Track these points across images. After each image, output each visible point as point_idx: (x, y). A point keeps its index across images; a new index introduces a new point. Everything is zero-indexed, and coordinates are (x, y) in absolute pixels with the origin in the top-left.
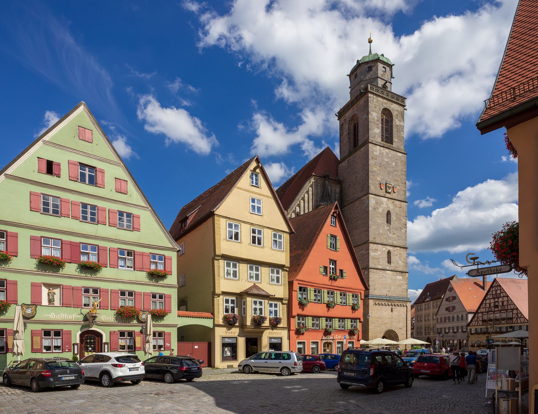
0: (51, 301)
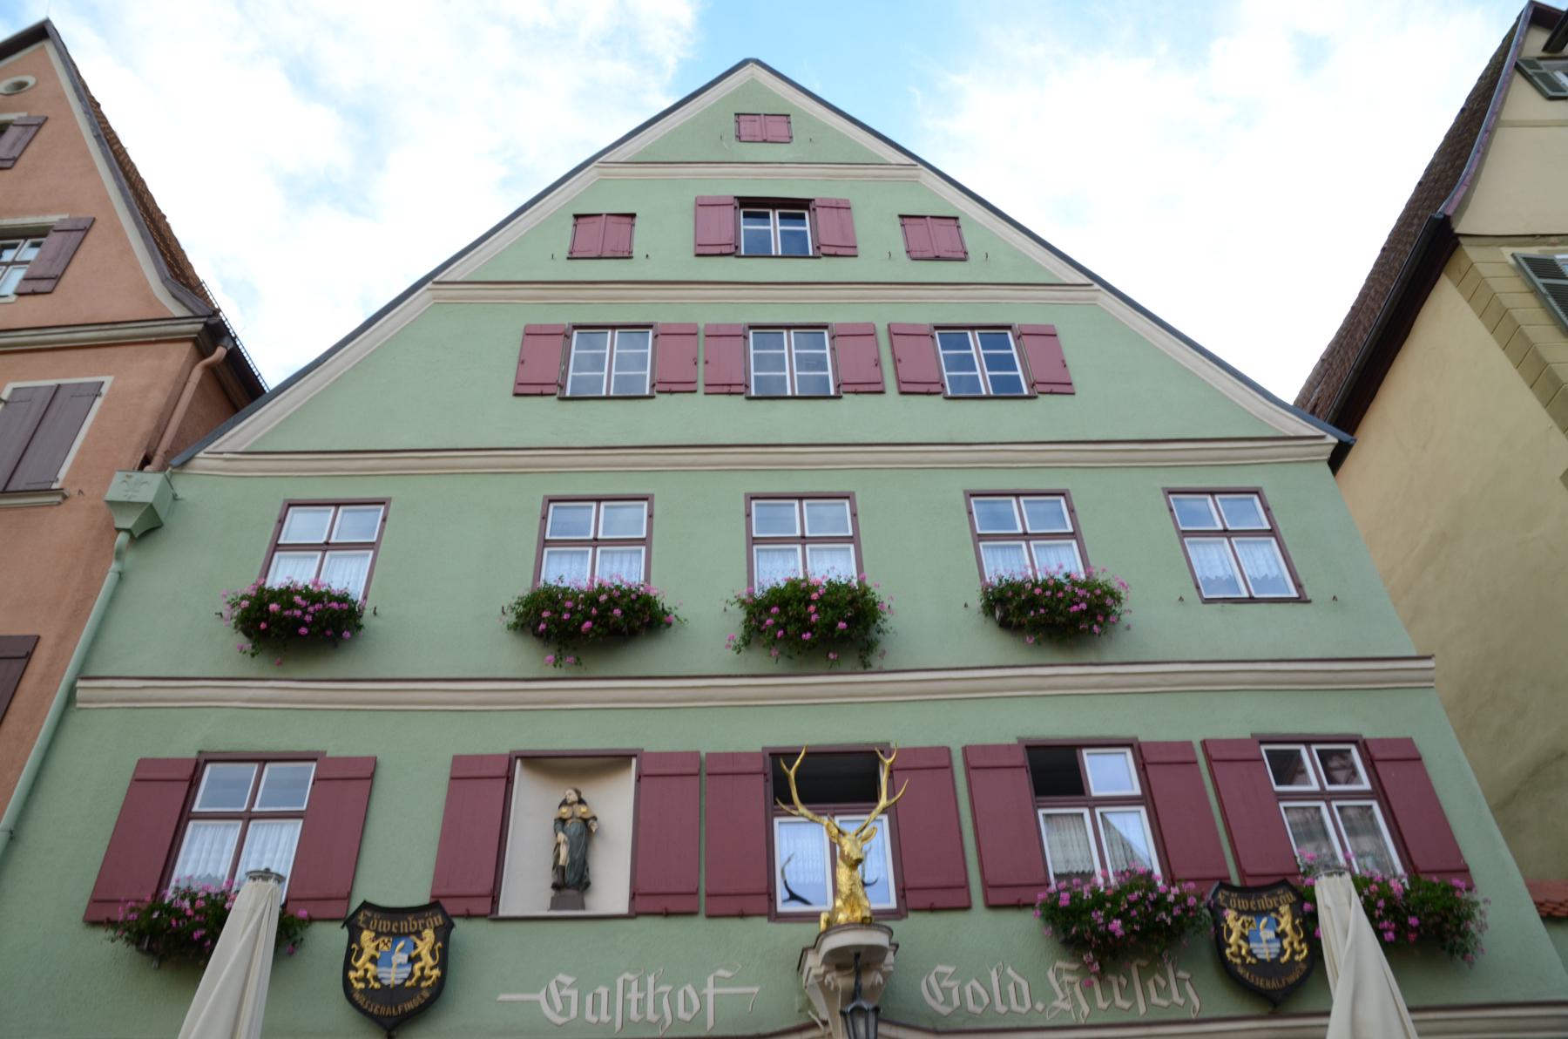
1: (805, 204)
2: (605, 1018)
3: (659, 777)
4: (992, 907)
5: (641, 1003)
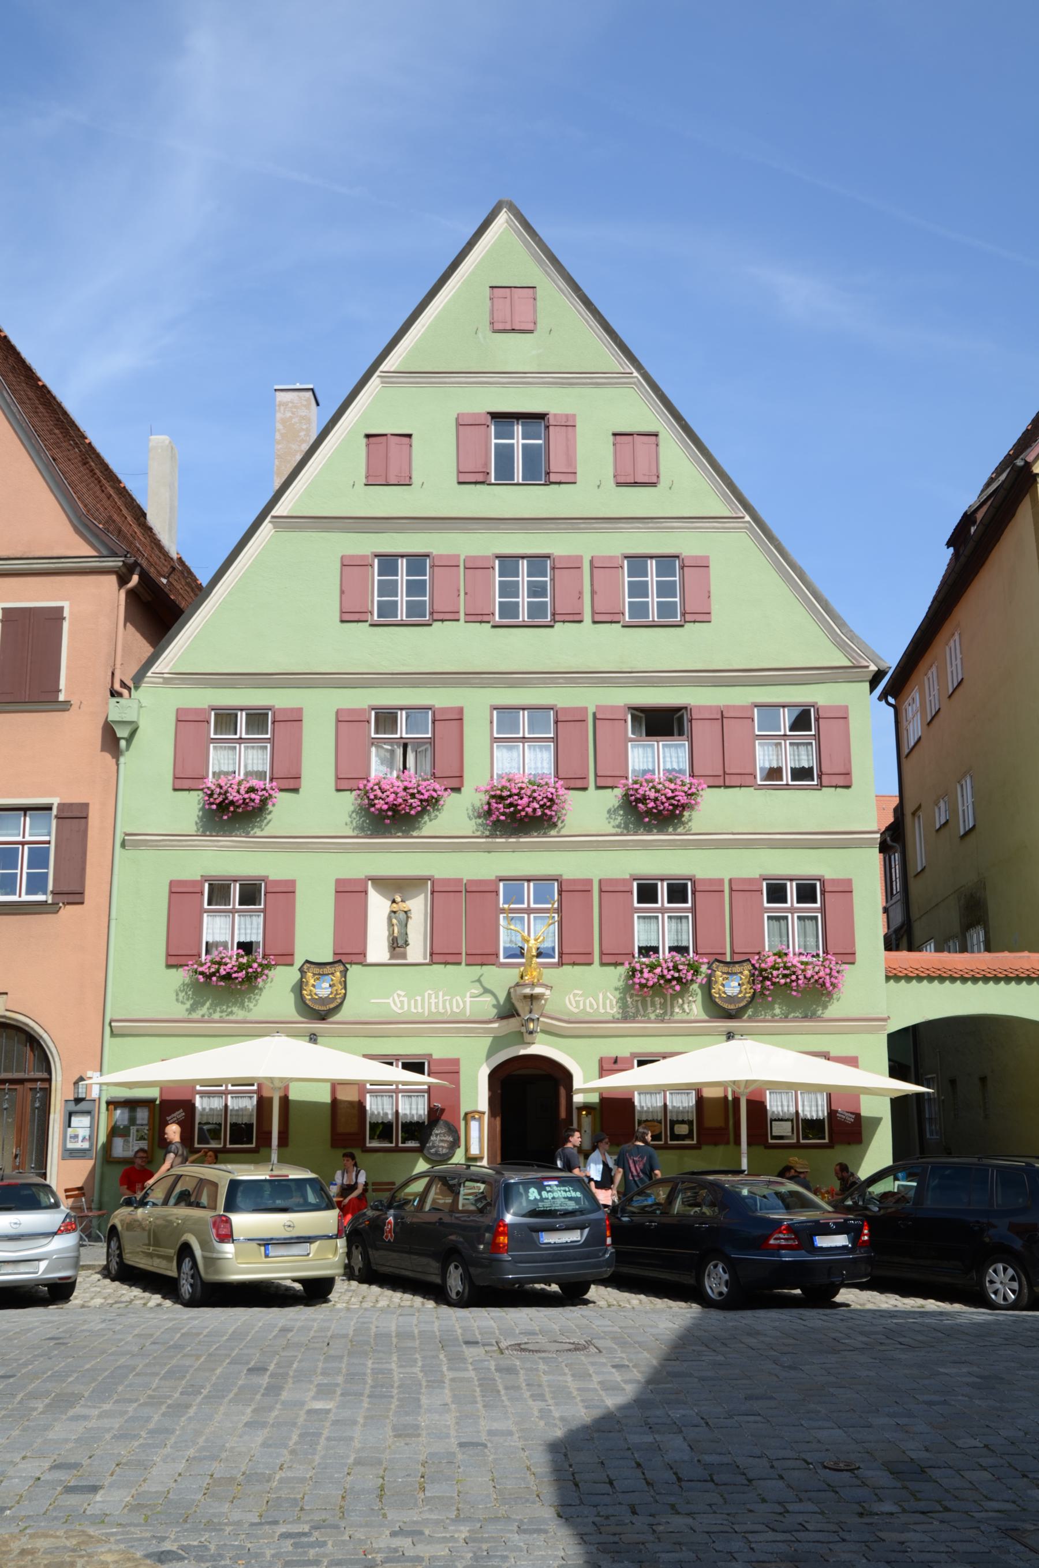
0: (397, 945)
1: (541, 417)
2: (420, 1010)
3: (441, 891)
4: (603, 964)
5: (437, 1004)
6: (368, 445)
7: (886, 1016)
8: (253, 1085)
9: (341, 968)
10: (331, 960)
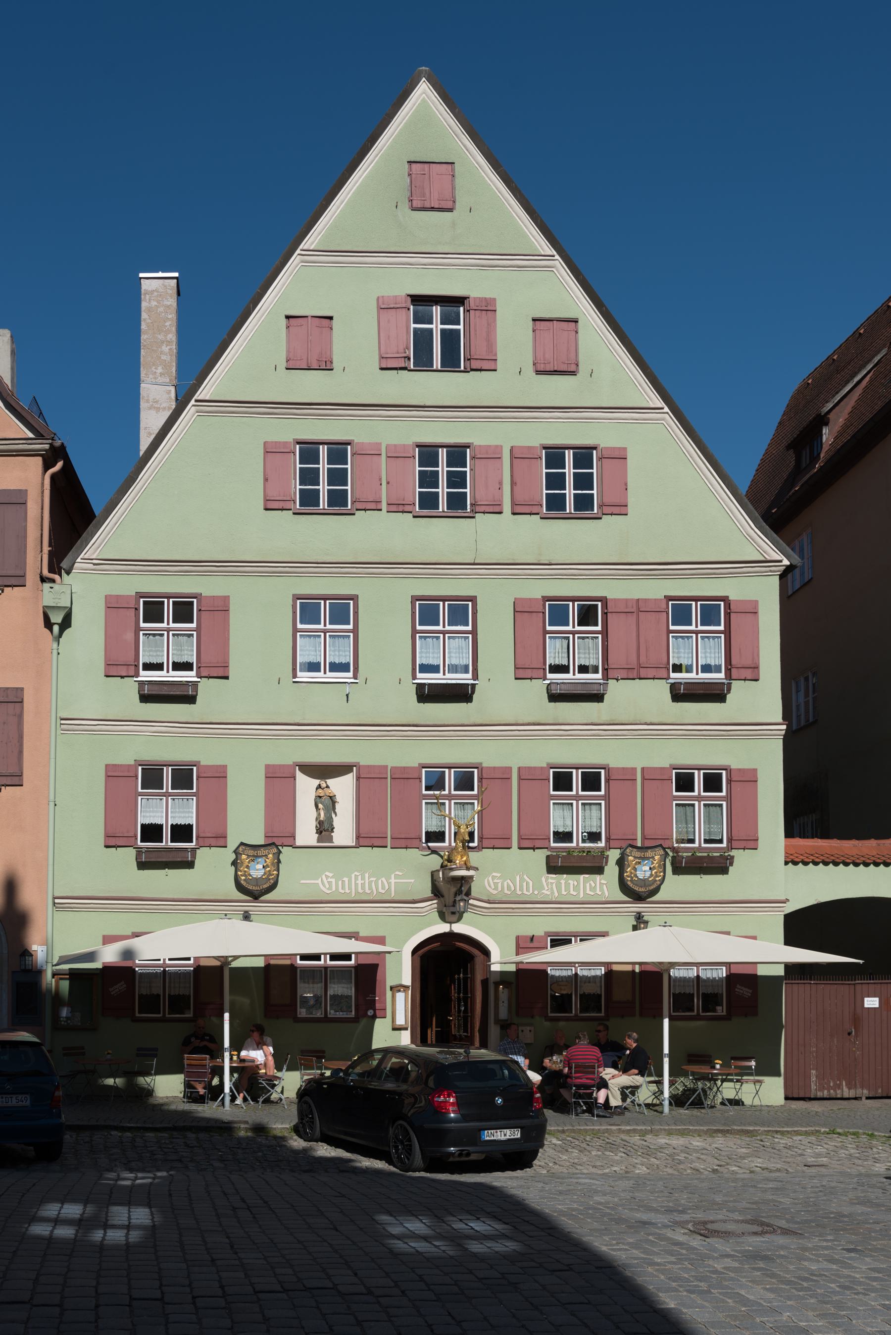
0: (324, 829)
1: (459, 301)
3: (368, 778)
5: (363, 885)
6: (288, 327)
7: (783, 898)
8: (189, 959)
9: (275, 850)
10: (262, 842)
